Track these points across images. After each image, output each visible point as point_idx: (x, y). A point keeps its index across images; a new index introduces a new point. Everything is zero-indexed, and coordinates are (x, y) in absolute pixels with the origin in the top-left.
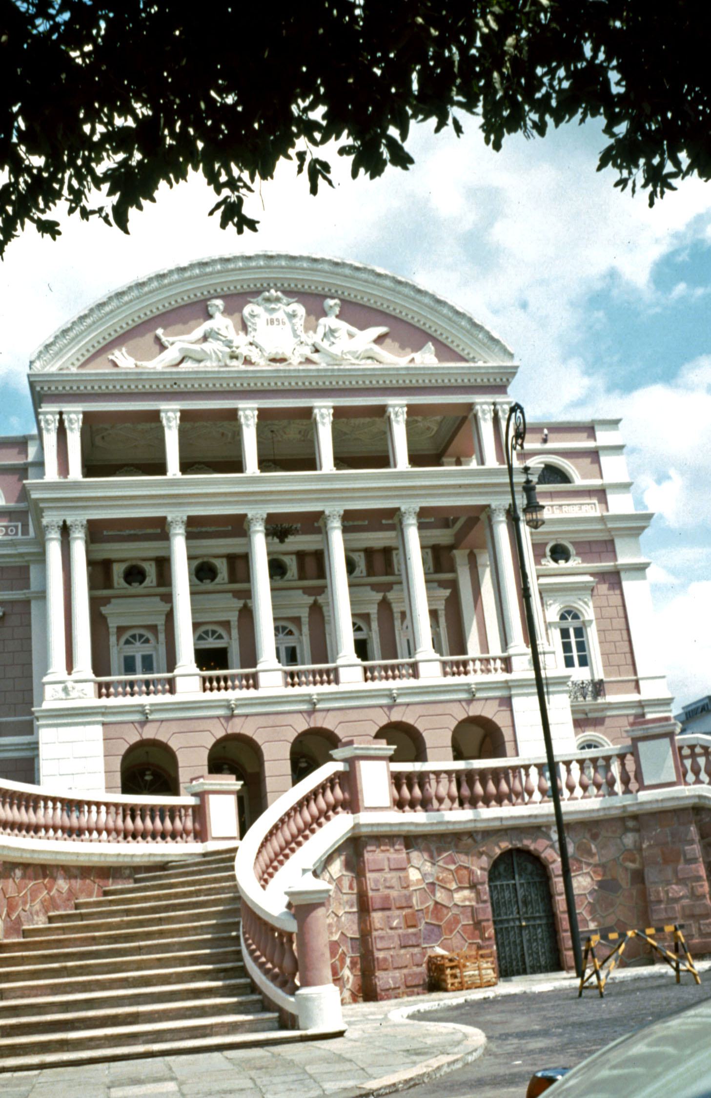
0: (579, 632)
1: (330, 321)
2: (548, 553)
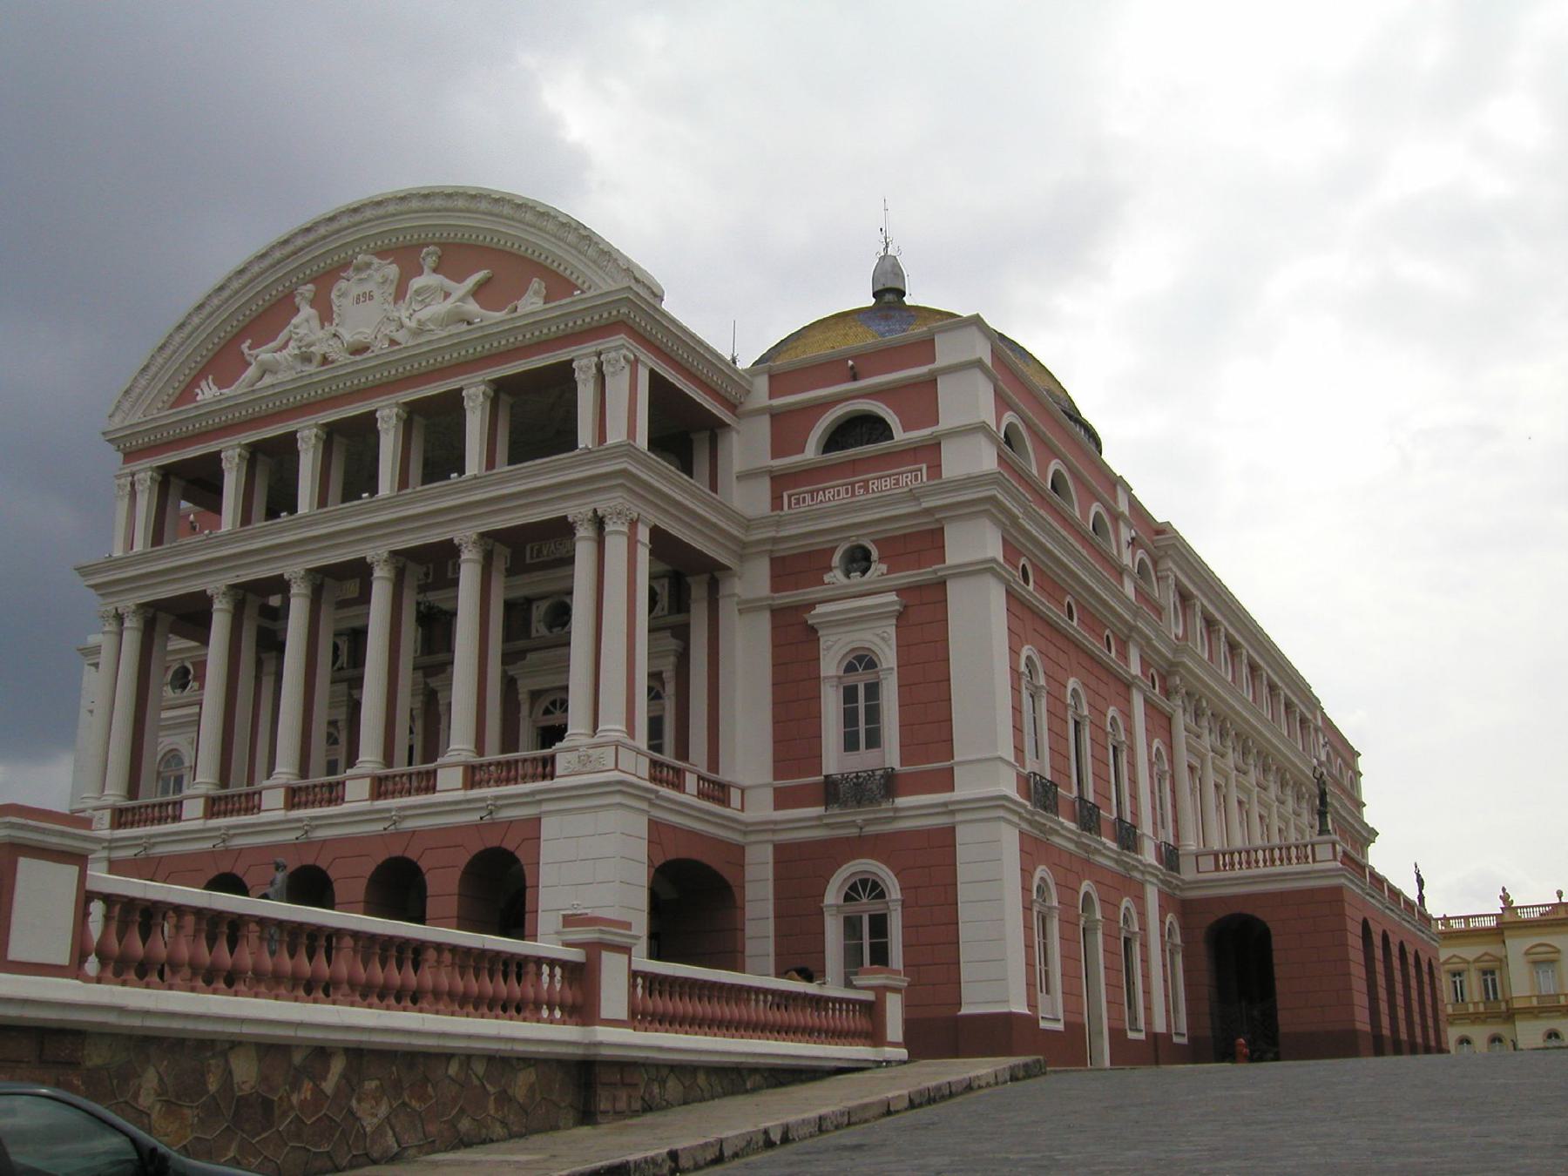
0: (873, 690)
1: (427, 279)
2: (836, 559)
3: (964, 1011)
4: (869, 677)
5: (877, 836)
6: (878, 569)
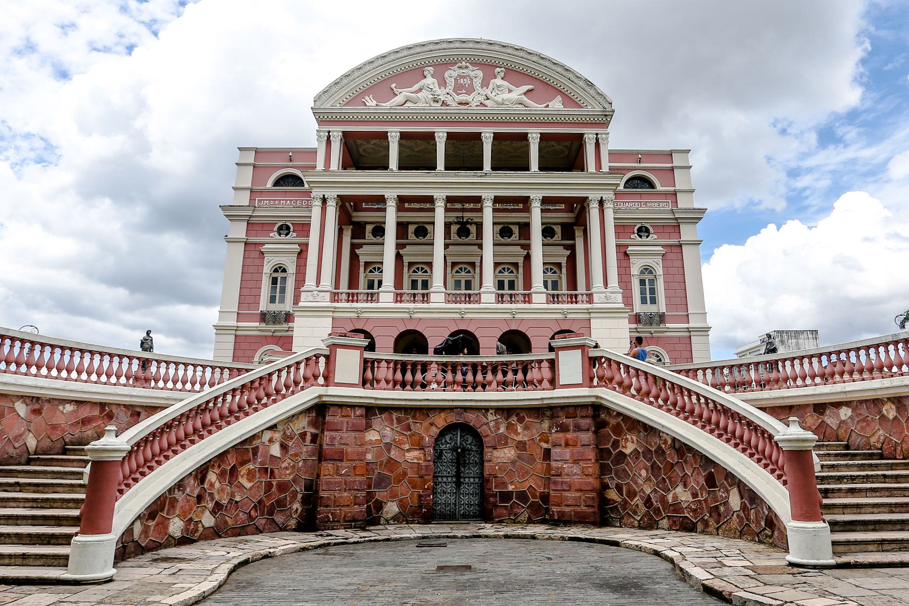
0: (652, 282)
1: (498, 81)
4: (651, 277)
6: (653, 237)
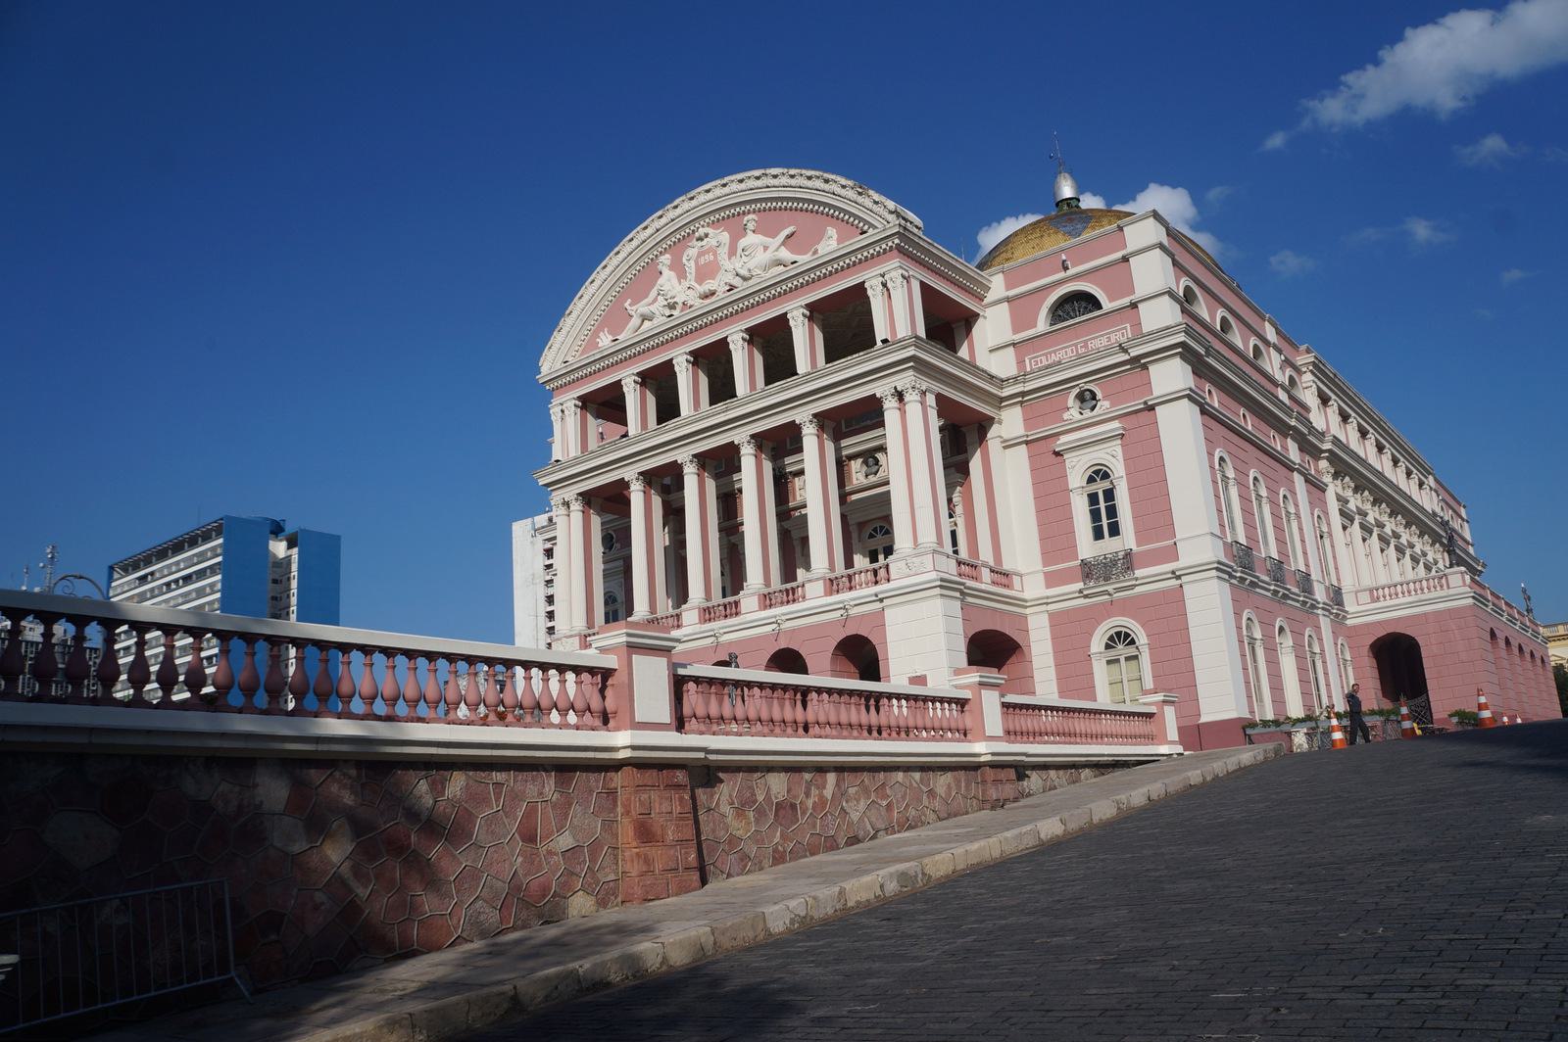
0: (1109, 495)
1: (750, 239)
3: (1204, 719)
4: (1106, 485)
5: (1124, 600)
6: (1104, 406)
